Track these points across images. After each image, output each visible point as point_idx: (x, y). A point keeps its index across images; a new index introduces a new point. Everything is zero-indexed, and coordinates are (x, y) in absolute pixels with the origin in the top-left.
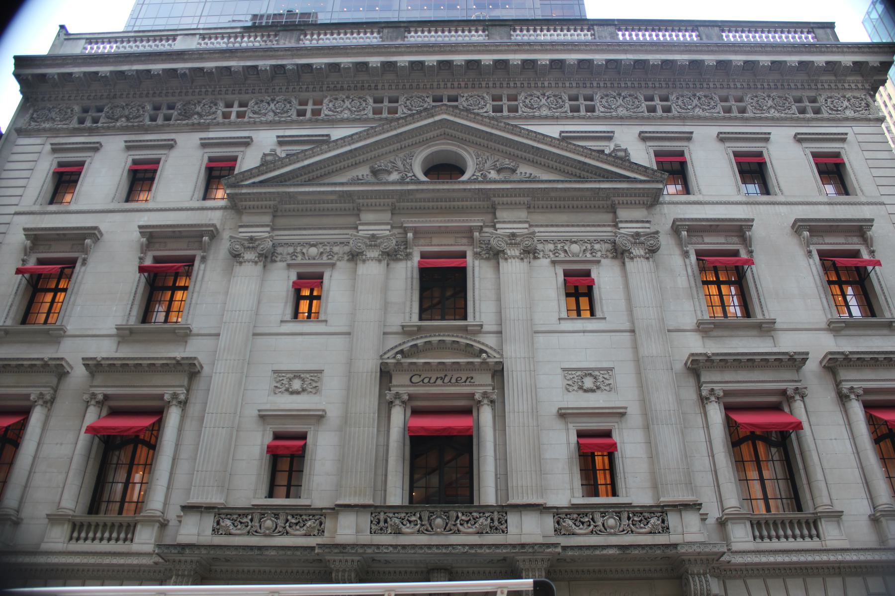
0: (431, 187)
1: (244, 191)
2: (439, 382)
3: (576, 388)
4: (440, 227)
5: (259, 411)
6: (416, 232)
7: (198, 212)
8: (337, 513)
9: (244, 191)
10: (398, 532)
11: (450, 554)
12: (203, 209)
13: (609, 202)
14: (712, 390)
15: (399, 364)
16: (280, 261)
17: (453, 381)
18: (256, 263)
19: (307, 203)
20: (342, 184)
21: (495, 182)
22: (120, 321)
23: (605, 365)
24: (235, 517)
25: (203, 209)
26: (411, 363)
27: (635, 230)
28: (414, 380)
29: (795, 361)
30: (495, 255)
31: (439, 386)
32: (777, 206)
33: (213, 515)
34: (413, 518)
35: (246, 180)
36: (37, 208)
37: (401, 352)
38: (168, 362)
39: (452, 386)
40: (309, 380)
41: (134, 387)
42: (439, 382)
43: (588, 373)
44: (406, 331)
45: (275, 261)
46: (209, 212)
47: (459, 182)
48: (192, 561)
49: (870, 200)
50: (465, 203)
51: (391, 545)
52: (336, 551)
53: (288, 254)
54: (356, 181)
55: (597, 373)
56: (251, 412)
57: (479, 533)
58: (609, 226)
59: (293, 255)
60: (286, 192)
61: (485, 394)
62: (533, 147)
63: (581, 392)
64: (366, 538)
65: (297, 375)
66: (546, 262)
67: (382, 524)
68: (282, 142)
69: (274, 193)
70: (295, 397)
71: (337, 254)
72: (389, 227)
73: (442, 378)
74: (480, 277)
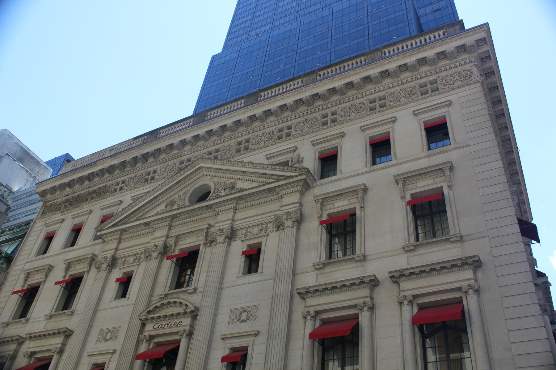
1: (104, 232)
2: (166, 326)
3: (236, 320)
5: (221, 336)
9: (104, 232)
12: (94, 245)
14: (308, 312)
17: (172, 325)
21: (223, 196)
22: (48, 312)
23: (255, 303)
25: (94, 245)
27: (286, 211)
31: (166, 329)
32: (389, 169)
36: (34, 258)
42: (166, 326)
47: (208, 201)
49: (460, 145)
55: (250, 309)
63: (238, 322)
73: (168, 324)
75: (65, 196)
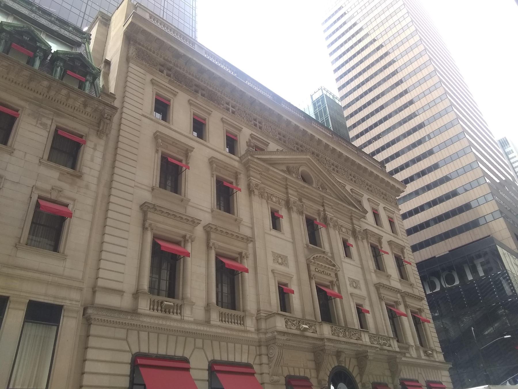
75: (164, 59)
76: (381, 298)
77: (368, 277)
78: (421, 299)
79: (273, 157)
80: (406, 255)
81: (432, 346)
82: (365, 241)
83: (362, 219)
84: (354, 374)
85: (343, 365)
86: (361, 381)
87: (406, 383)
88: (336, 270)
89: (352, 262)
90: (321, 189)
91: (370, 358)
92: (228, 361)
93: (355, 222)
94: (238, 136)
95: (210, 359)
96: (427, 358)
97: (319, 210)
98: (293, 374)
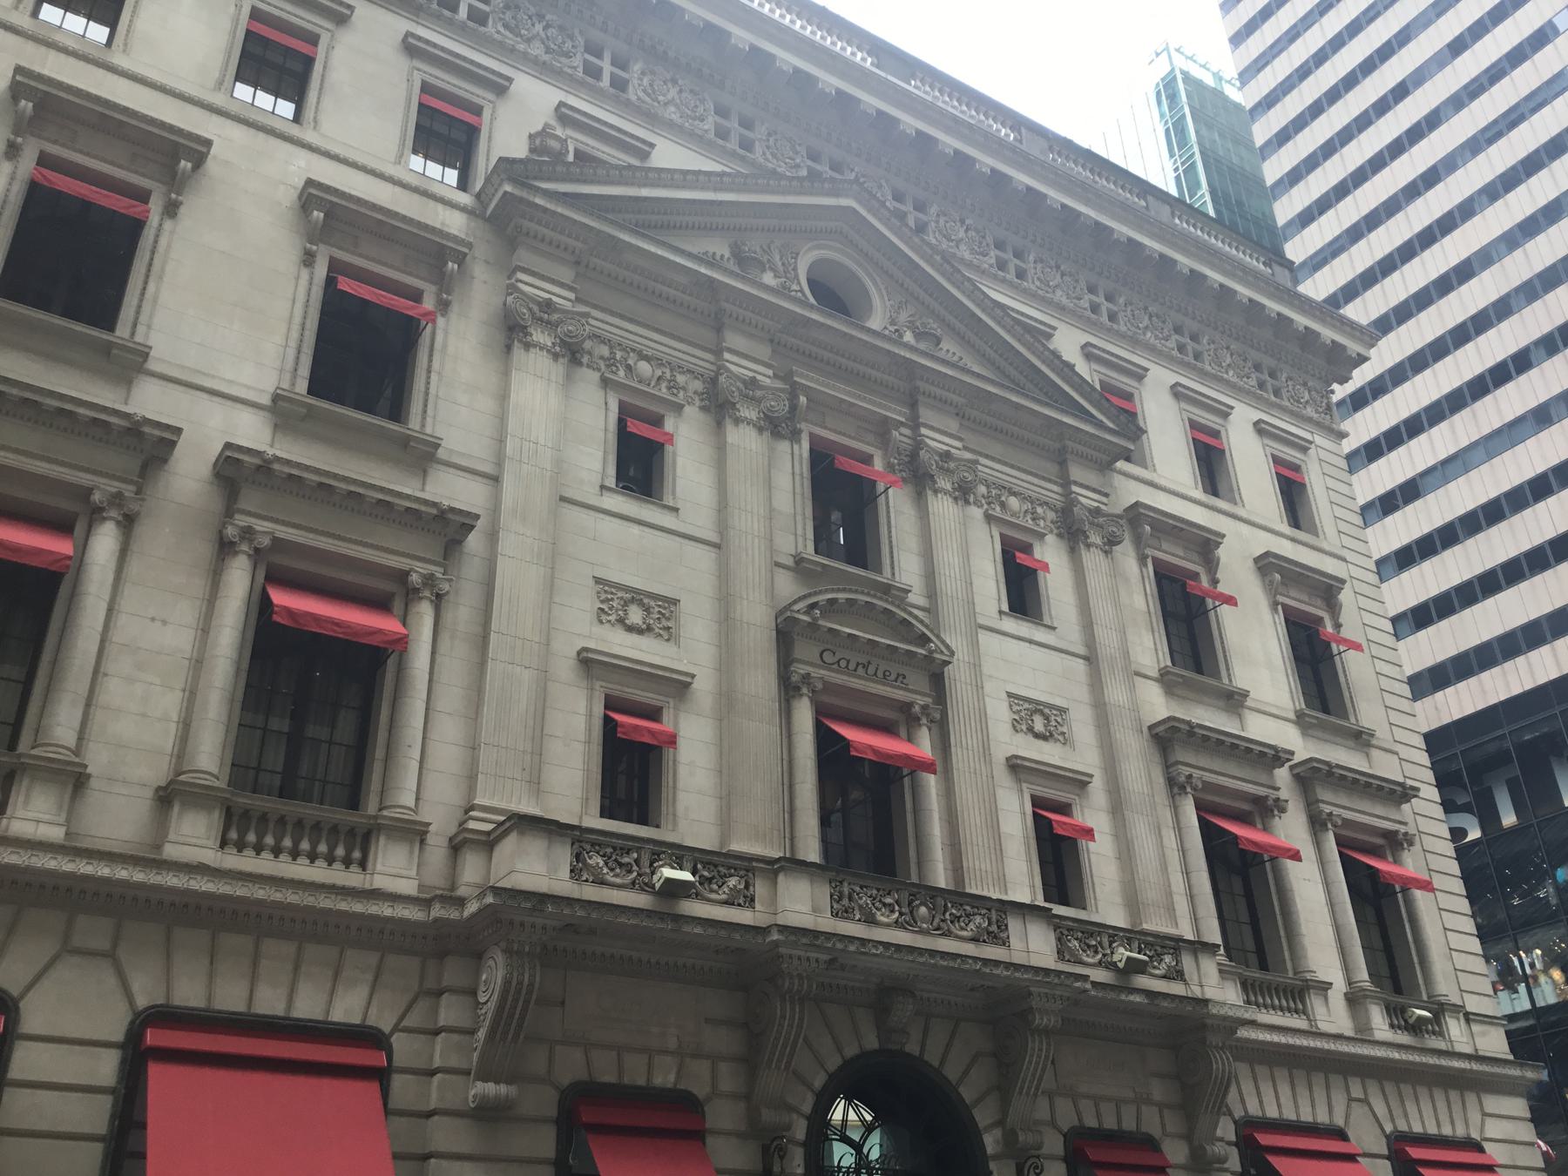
0: (815, 316)
2: (861, 671)
4: (843, 401)
6: (815, 399)
7: (416, 197)
8: (776, 873)
10: (870, 920)
11: (959, 970)
13: (1057, 445)
15: (813, 626)
16: (588, 366)
17: (880, 674)
18: (556, 356)
19: (663, 283)
20: (690, 256)
24: (609, 850)
26: (830, 630)
28: (828, 657)
29: (1273, 757)
30: (919, 479)
31: (859, 677)
33: (569, 841)
34: (888, 900)
35: (542, 179)
37: (813, 606)
38: (423, 508)
39: (837, 672)
40: (659, 614)
41: (339, 538)
43: (1038, 708)
44: (799, 566)
45: (580, 364)
46: (440, 207)
48: (544, 928)
50: (874, 373)
51: (881, 943)
52: (804, 941)
53: (602, 358)
54: (711, 262)
56: (566, 650)
57: (974, 940)
58: (1055, 483)
59: (611, 363)
60: (614, 237)
61: (924, 707)
62: (973, 315)
64: (827, 923)
65: (637, 597)
66: (977, 513)
67: (845, 902)
68: (564, 114)
69: (591, 228)
70: (634, 638)
71: (684, 388)
72: (770, 373)
74: (897, 508)
76: (1175, 786)
77: (1116, 693)
78: (1401, 794)
79: (645, 192)
80: (1349, 615)
81: (1445, 987)
82: (1126, 555)
83: (1121, 464)
84: (967, 1093)
85: (913, 1048)
86: (1000, 1123)
87: (1265, 1139)
88: (929, 658)
89: (1040, 635)
90: (908, 337)
91: (1040, 1021)
92: (167, 1006)
93: (1076, 472)
94: (486, 114)
95: (142, 1002)
96: (1403, 1038)
97: (885, 421)
98: (609, 1078)
